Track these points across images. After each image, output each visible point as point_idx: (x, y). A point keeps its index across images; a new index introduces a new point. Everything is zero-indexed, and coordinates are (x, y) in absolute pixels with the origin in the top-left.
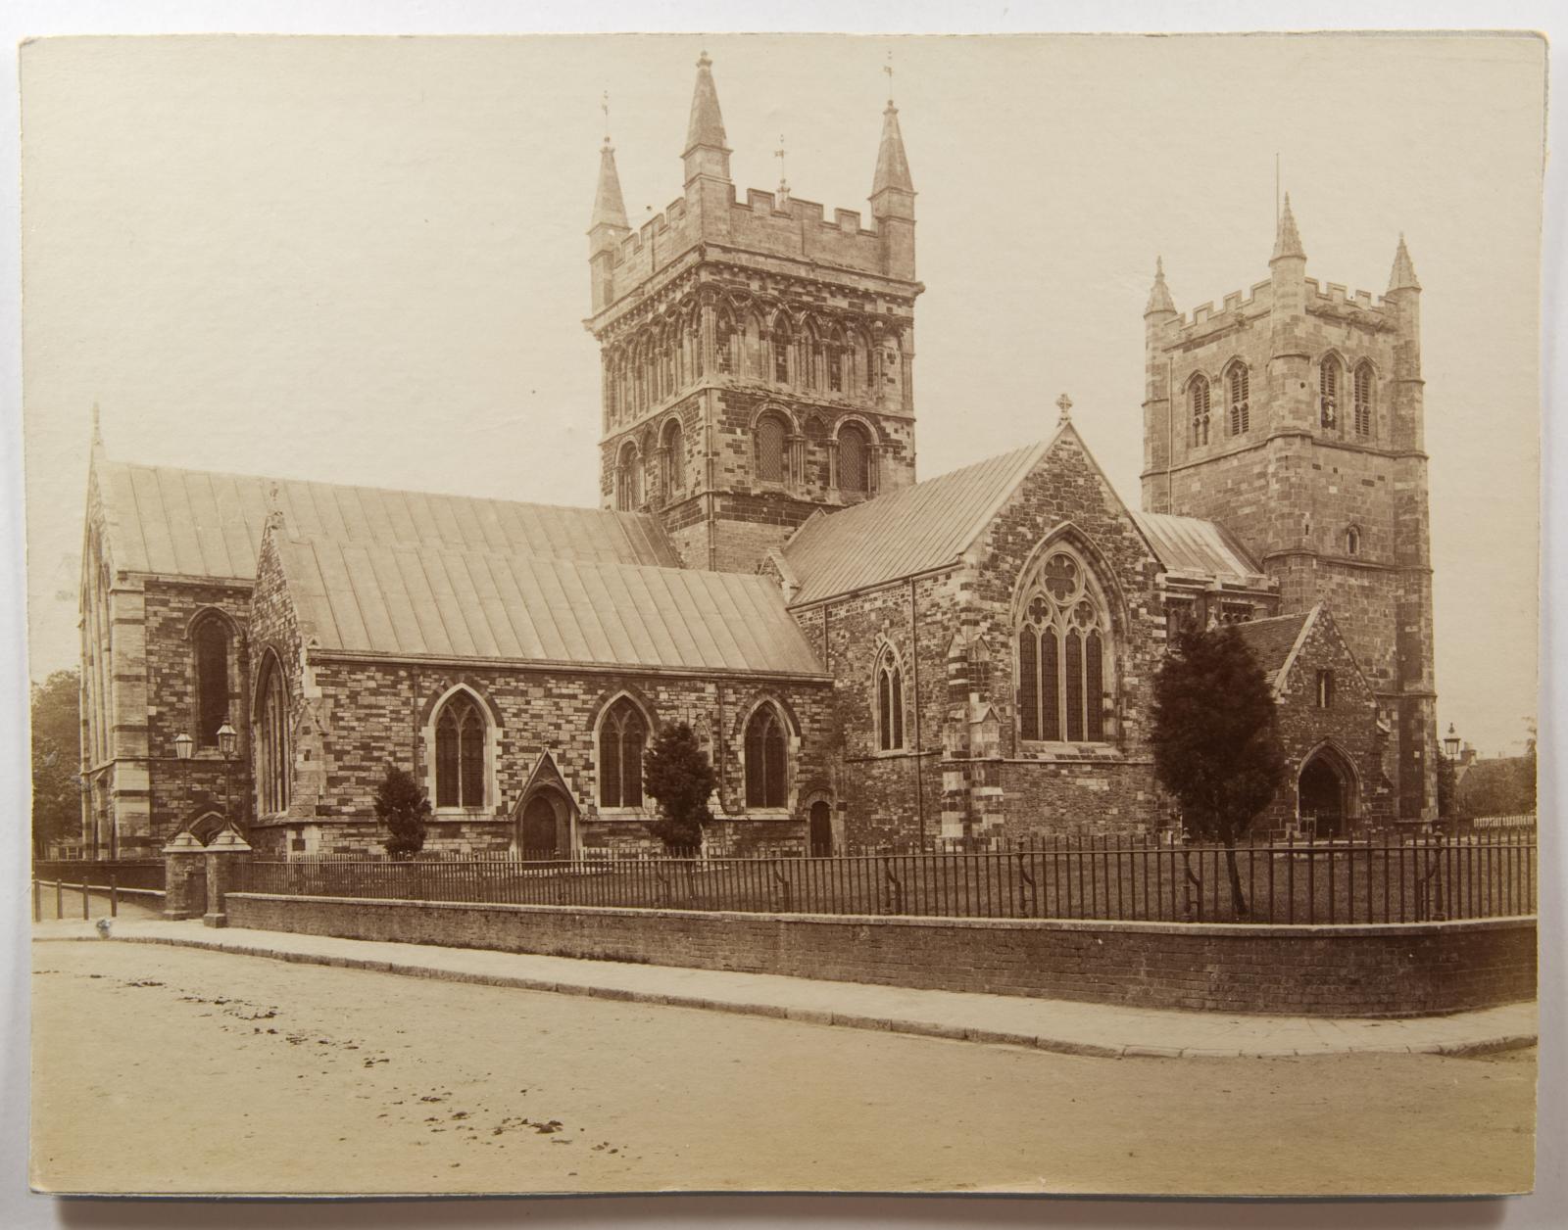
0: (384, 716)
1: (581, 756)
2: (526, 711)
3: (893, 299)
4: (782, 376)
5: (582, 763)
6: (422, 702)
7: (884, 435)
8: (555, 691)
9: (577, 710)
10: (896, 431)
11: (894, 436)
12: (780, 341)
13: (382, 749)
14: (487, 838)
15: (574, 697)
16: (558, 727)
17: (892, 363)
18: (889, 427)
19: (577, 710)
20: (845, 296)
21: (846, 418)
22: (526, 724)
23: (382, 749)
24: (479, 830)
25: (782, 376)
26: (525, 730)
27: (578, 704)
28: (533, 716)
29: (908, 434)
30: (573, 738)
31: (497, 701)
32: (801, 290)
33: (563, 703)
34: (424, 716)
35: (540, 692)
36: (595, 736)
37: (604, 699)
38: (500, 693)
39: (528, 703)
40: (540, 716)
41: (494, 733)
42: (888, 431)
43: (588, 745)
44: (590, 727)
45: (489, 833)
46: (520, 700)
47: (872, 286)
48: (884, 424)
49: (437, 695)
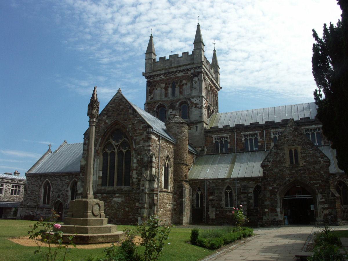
0: (35, 186)
1: (65, 194)
2: (57, 184)
3: (195, 68)
4: (166, 95)
5: (66, 195)
6: (41, 183)
7: (192, 102)
8: (62, 179)
9: (66, 183)
10: (196, 101)
11: (195, 102)
12: (166, 88)
13: (34, 193)
14: (48, 211)
15: (65, 180)
16: (62, 187)
17: (195, 84)
18: (193, 100)
19: (66, 183)
20: (182, 72)
21: (180, 101)
22: (57, 187)
23: (34, 193)
24: (46, 209)
25: (166, 95)
26: (56, 188)
27: (66, 182)
28: (58, 185)
29: (200, 100)
30: (64, 190)
31: (53, 182)
32: (170, 75)
33: (63, 182)
34: (41, 186)
35: (60, 180)
36: (69, 189)
37: (71, 180)
38: (53, 180)
39: (57, 182)
40: (59, 185)
41: (52, 189)
42: (193, 101)
43: (67, 191)
44: (68, 186)
45: (48, 210)
46: (56, 182)
47: (188, 67)
48: (191, 100)
49: (43, 181)
